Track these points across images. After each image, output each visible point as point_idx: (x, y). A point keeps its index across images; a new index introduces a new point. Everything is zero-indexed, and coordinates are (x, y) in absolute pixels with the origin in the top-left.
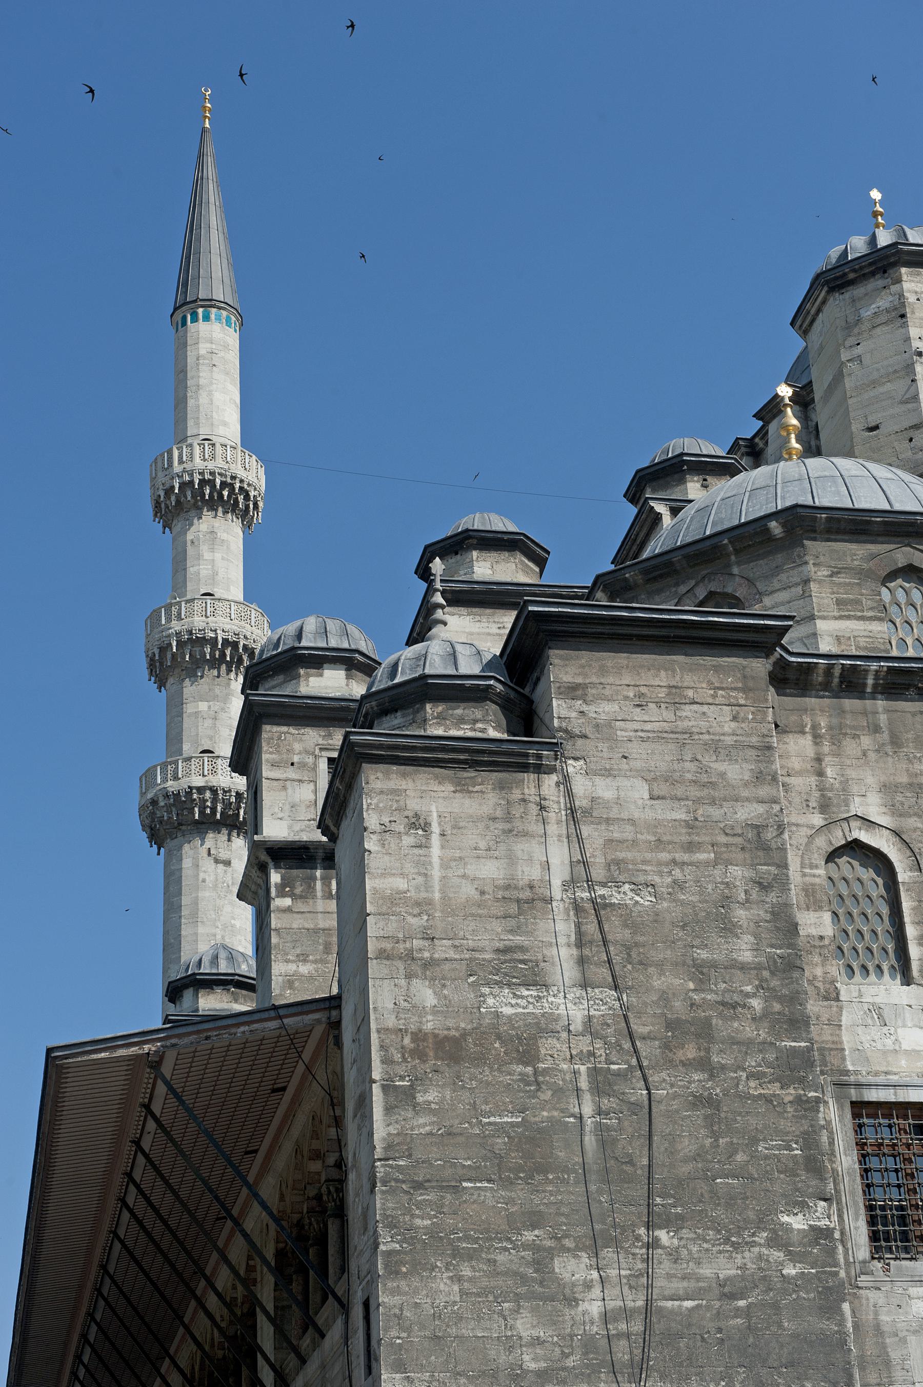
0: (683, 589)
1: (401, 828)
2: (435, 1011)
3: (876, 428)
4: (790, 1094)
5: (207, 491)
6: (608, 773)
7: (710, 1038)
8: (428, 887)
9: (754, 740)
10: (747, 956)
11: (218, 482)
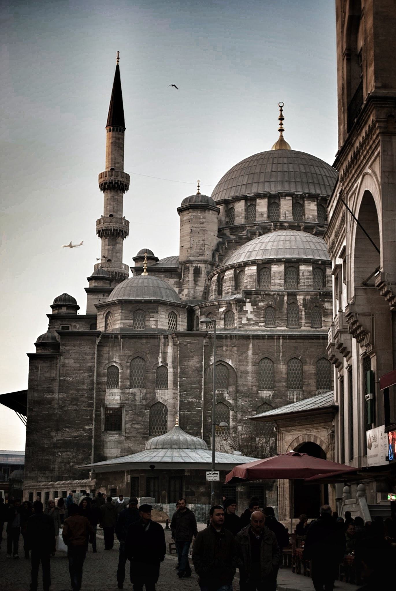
0: (105, 309)
1: (34, 368)
2: (37, 397)
3: (183, 246)
4: (89, 409)
5: (111, 185)
6: (68, 359)
7: (78, 401)
8: (38, 378)
9: (92, 352)
10: (85, 388)
11: (114, 182)
